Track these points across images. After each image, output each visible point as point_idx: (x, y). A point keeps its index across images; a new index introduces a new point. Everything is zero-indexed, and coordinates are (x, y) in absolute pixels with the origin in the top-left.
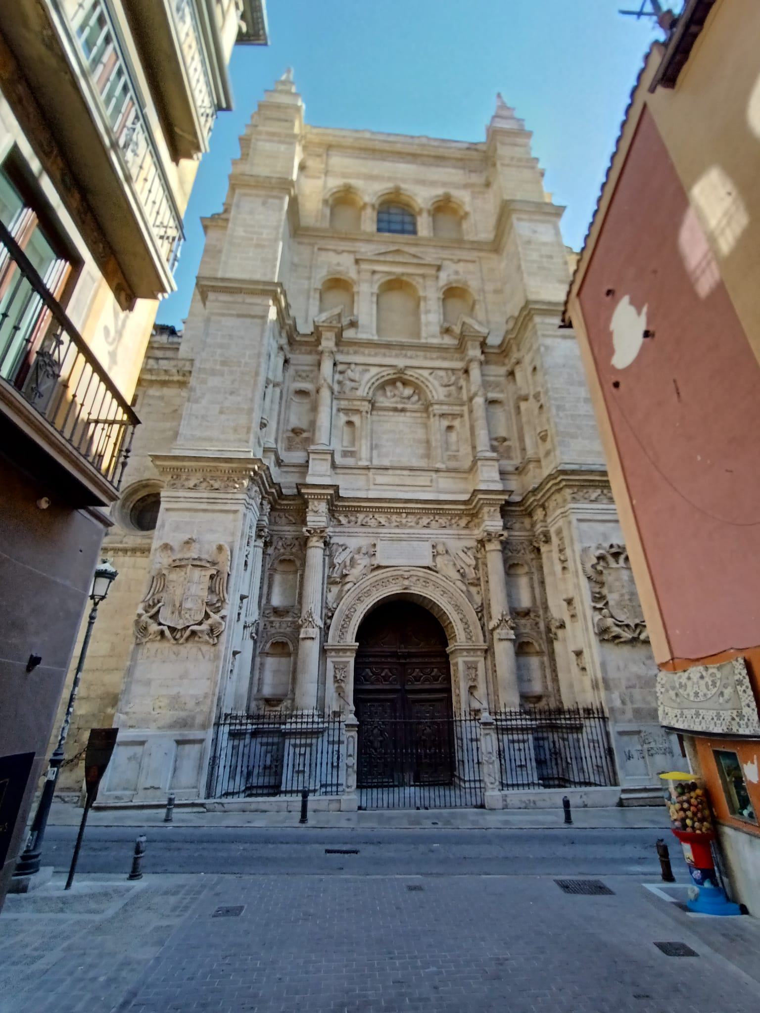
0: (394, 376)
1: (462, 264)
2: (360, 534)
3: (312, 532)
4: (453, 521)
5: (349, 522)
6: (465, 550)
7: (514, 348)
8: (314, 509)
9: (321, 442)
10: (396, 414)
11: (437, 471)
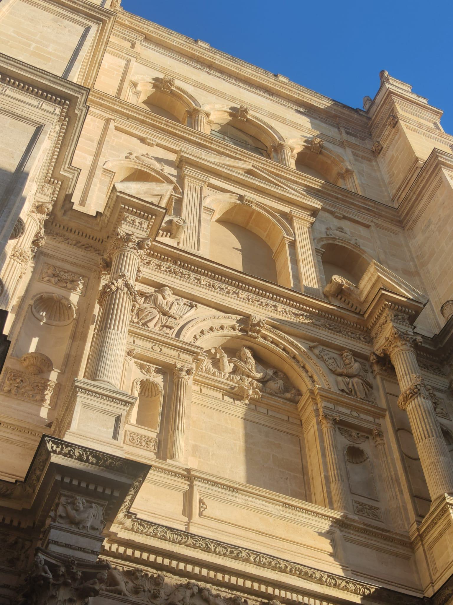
1: (348, 223)
3: (63, 569)
8: (73, 513)
9: (108, 380)
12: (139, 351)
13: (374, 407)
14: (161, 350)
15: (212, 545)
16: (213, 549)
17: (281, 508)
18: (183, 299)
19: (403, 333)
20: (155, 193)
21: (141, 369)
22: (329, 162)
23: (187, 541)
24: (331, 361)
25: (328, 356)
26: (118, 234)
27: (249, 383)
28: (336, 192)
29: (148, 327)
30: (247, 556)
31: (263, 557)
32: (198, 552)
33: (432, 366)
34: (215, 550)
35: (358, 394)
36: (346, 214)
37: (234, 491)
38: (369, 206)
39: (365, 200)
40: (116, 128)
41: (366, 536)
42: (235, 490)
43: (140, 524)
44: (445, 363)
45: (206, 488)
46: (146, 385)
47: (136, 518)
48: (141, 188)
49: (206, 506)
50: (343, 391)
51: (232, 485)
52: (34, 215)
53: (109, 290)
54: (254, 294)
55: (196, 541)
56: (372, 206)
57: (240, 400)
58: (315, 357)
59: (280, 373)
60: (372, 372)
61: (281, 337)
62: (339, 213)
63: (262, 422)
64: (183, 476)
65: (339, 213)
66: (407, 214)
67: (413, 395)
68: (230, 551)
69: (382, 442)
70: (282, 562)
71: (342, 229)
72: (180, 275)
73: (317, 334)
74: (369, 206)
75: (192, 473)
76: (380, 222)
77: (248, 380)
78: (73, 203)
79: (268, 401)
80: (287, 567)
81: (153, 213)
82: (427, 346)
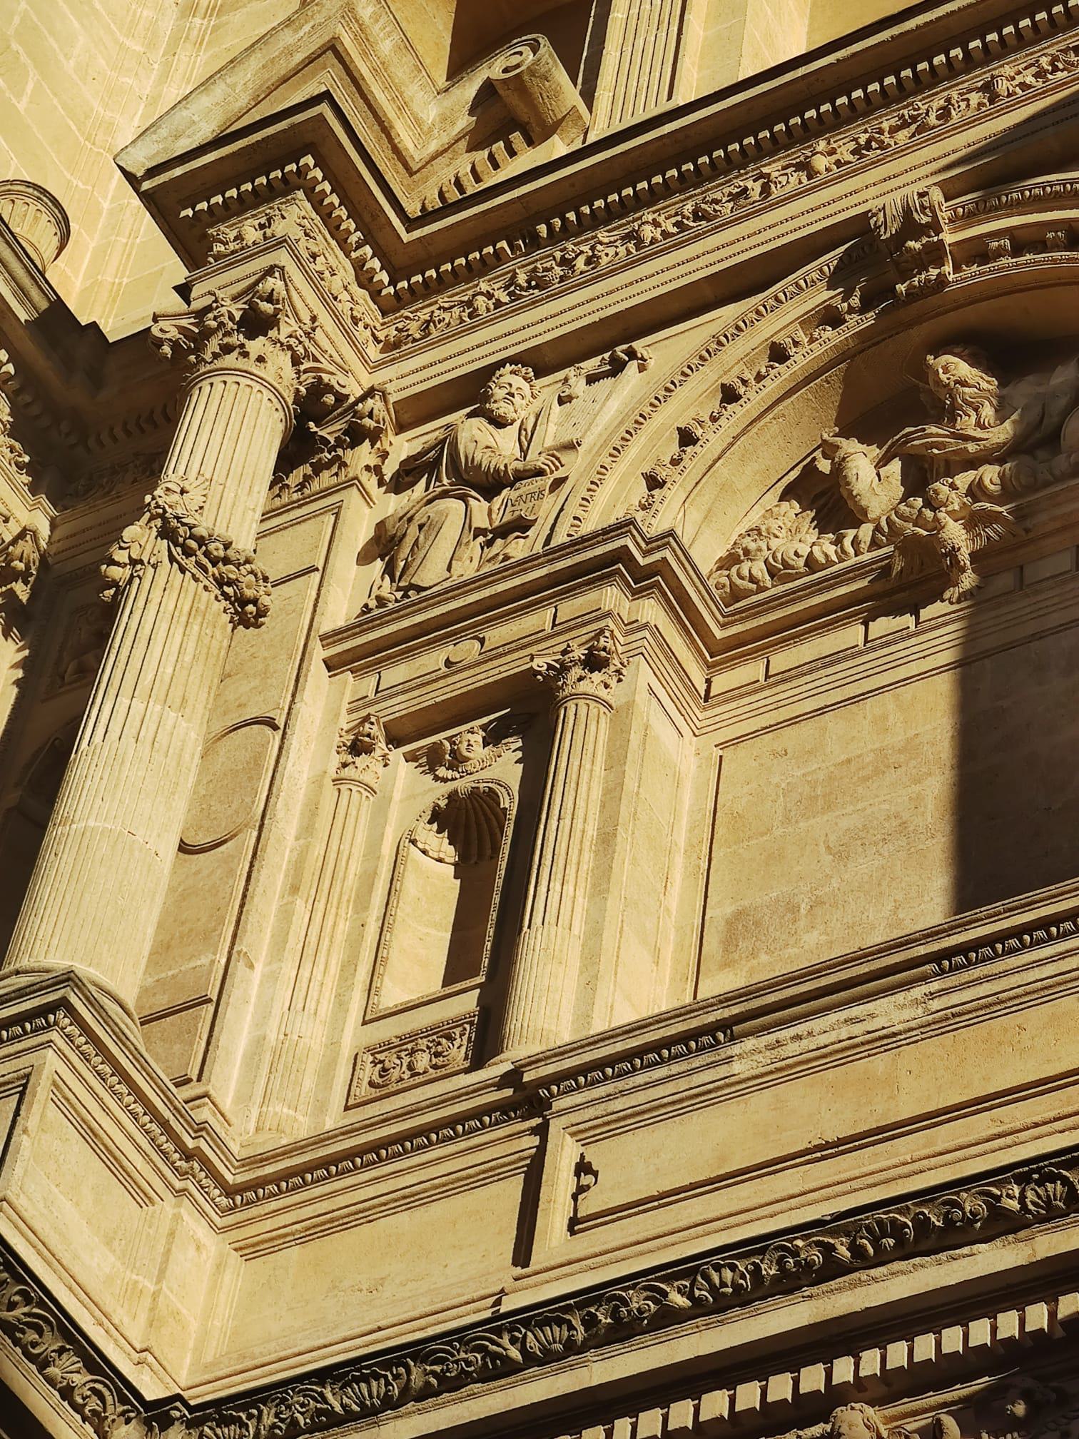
12: (399, 707)
14: (482, 641)
15: (505, 1340)
16: (515, 1353)
17: (935, 986)
18: (582, 365)
20: (299, 57)
21: (432, 770)
23: (409, 1380)
26: (159, 343)
27: (970, 492)
29: (419, 589)
30: (656, 1301)
31: (718, 1268)
32: (473, 1396)
34: (523, 1351)
37: (718, 1042)
42: (721, 1036)
43: (225, 1421)
45: (600, 1101)
46: (472, 812)
47: (191, 1409)
48: (234, 85)
49: (596, 1174)
51: (694, 1024)
53: (112, 591)
54: (887, 106)
55: (441, 1361)
57: (937, 596)
61: (1037, 199)
63: (1055, 619)
64: (505, 1110)
68: (584, 1322)
70: (800, 1243)
72: (558, 271)
75: (526, 1078)
77: (953, 487)
79: (1058, 512)
80: (828, 1249)
81: (289, 146)
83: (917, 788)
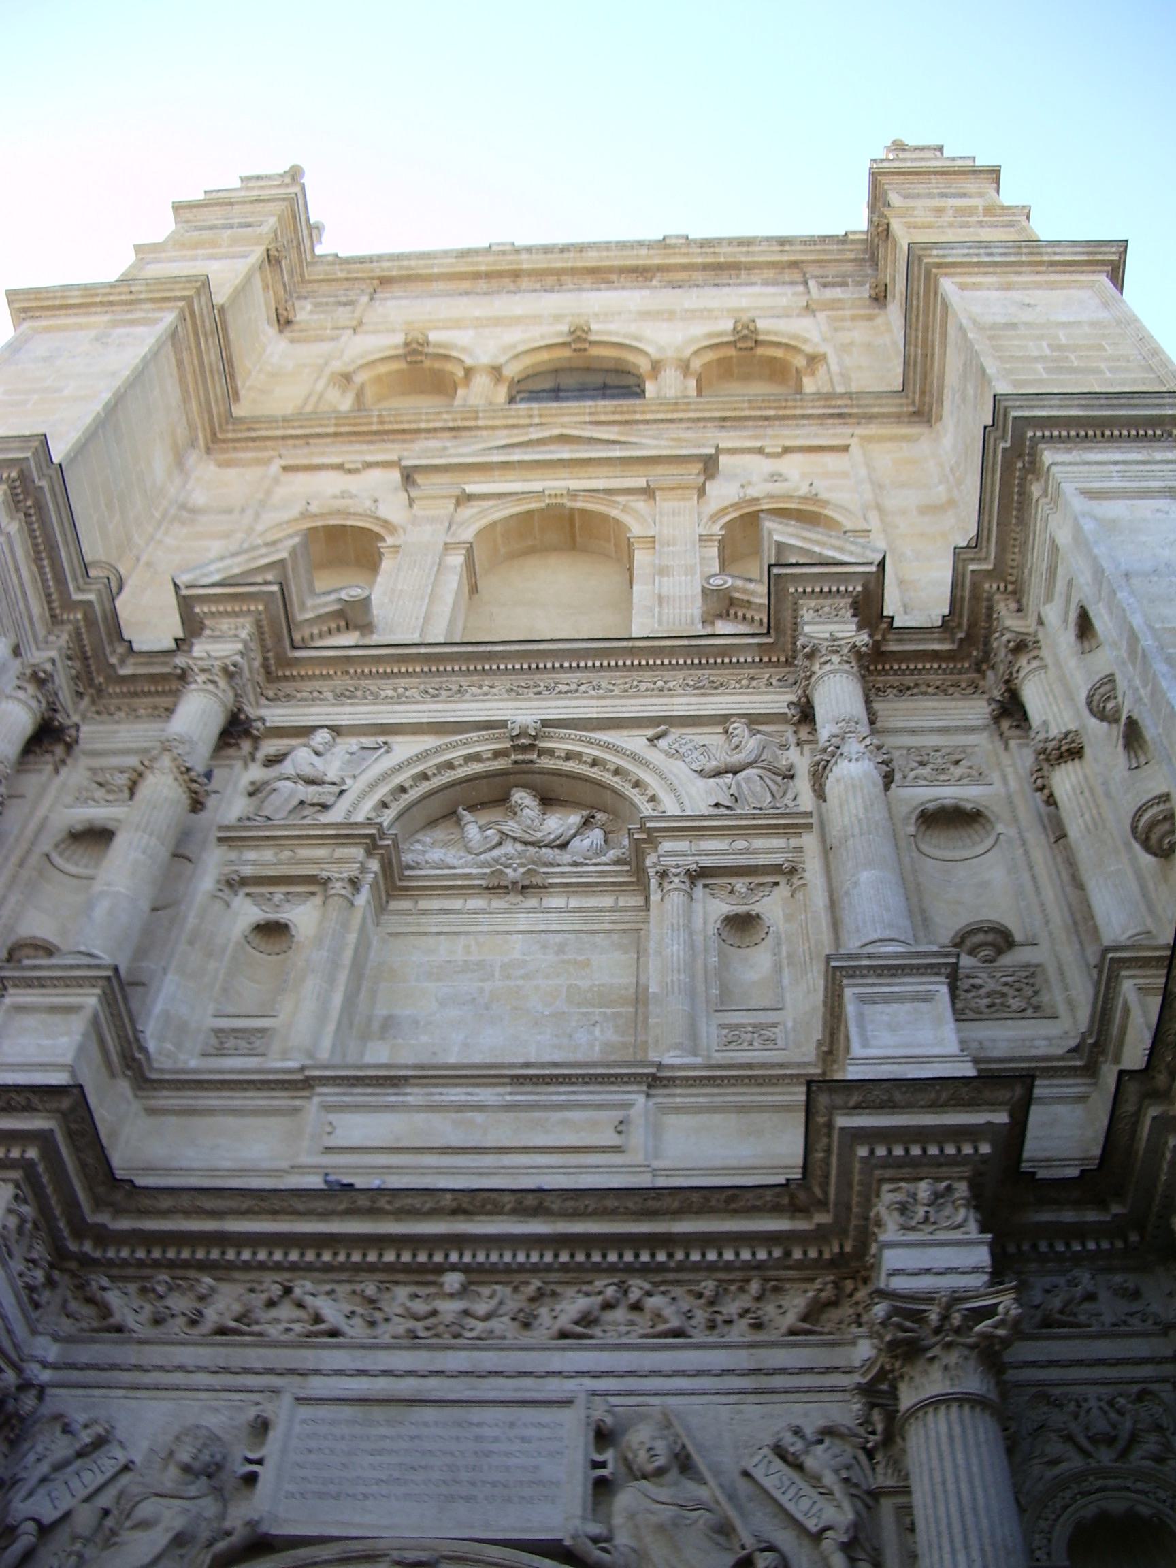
0: (498, 765)
2: (203, 1379)
4: (731, 1308)
5: (157, 1321)
6: (795, 1446)
7: (1005, 611)
10: (498, 903)
11: (656, 1081)
12: (247, 871)
13: (782, 815)
17: (509, 1089)
19: (826, 639)
22: (778, 353)
24: (696, 754)
25: (689, 746)
28: (760, 408)
33: (956, 685)
35: (750, 800)
36: (788, 443)
38: (839, 407)
39: (826, 399)
40: (286, 469)
41: (716, 1090)
44: (984, 667)
50: (717, 805)
52: (21, 694)
56: (846, 406)
58: (662, 756)
59: (599, 816)
60: (798, 744)
62: (773, 446)
63: (554, 927)
65: (773, 446)
66: (923, 393)
67: (828, 762)
69: (801, 882)
71: (780, 475)
73: (665, 708)
74: (839, 407)
76: (872, 429)
78: (130, 642)
82: (936, 647)
83: (481, 984)
